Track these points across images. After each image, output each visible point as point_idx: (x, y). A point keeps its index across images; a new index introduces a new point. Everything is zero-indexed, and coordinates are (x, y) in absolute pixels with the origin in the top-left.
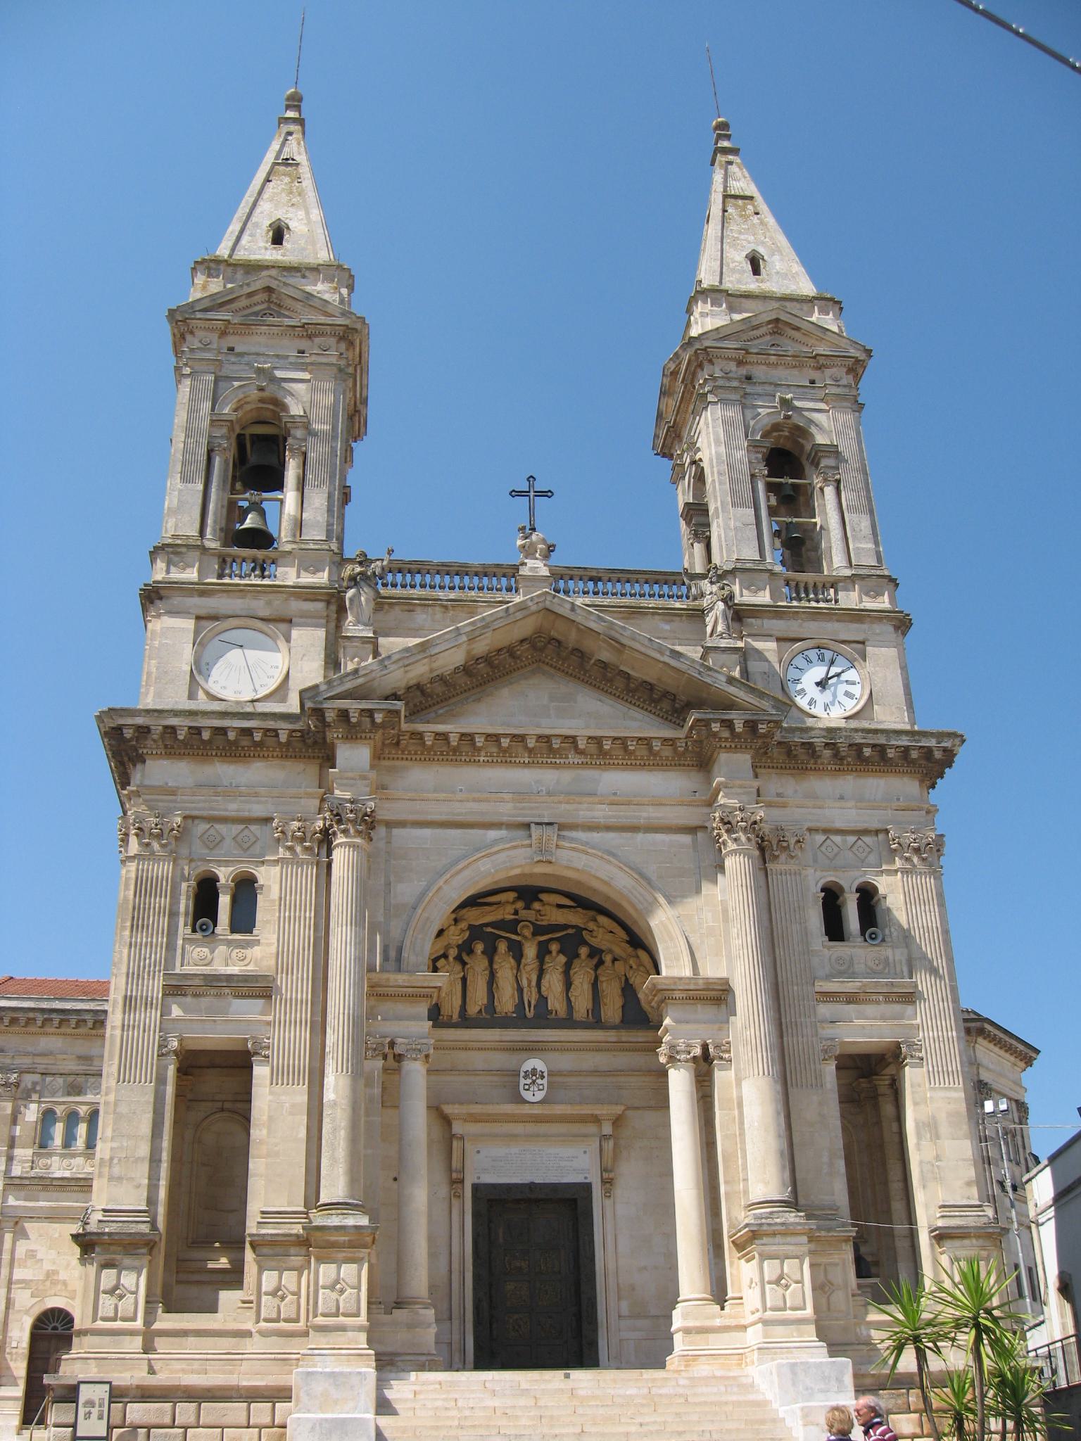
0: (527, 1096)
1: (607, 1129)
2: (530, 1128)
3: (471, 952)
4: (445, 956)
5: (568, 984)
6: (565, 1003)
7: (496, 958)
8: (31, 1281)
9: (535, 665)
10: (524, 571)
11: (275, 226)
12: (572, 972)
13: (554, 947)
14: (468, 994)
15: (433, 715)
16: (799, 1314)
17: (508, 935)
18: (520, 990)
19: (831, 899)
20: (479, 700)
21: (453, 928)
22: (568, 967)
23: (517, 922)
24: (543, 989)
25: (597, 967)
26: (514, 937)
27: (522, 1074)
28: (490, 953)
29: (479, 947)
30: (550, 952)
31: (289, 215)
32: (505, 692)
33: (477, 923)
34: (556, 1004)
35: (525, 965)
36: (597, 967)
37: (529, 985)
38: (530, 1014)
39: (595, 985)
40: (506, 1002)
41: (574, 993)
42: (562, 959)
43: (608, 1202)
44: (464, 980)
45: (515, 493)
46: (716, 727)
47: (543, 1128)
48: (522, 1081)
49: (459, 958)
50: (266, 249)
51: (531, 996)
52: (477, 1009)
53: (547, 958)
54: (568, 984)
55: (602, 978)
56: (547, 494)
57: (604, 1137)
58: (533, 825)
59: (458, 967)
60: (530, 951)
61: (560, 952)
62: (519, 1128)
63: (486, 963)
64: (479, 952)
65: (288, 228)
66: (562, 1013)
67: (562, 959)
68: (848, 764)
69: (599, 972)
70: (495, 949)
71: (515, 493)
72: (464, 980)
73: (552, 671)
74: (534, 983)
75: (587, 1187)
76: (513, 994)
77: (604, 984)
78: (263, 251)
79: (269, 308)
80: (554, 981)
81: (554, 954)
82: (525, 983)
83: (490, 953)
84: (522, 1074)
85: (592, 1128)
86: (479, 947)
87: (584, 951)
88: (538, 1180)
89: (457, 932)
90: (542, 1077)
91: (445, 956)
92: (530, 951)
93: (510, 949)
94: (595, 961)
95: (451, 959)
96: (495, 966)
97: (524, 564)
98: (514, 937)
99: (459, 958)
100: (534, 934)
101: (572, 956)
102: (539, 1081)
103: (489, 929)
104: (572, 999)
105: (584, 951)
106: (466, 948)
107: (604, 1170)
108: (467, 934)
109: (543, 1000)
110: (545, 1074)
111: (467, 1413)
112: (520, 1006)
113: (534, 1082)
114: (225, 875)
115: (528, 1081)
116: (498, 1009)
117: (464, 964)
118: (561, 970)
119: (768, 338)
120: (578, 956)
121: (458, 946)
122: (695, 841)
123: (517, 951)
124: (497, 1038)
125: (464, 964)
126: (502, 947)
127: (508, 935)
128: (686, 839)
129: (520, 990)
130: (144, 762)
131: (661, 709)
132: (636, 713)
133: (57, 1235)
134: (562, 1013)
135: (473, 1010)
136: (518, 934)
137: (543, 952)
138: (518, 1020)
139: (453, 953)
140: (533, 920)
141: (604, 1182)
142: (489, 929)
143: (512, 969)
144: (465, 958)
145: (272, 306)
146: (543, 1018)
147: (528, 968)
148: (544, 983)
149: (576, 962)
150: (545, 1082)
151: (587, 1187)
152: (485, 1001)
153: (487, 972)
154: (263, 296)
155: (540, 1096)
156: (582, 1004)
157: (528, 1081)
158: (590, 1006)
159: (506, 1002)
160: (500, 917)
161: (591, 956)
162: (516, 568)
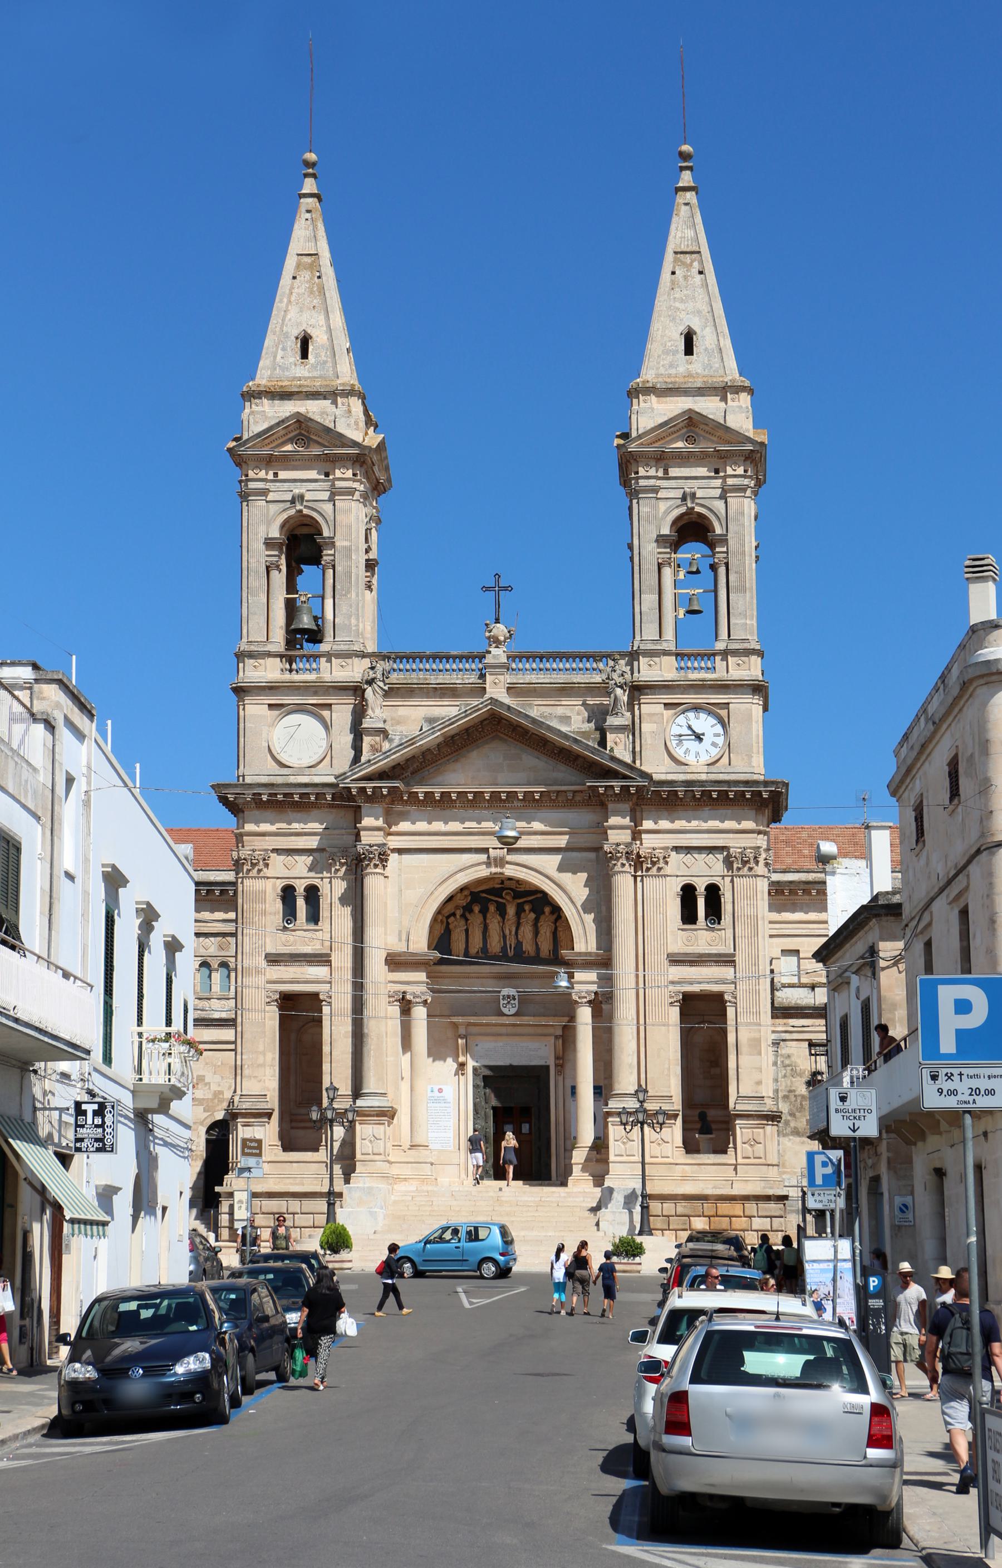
0: (505, 1011)
1: (559, 1032)
2: (510, 1030)
3: (471, 911)
4: (454, 914)
5: (536, 933)
6: (534, 946)
7: (488, 915)
8: (203, 1099)
9: (494, 734)
10: (489, 660)
11: (300, 337)
12: (539, 925)
13: (527, 907)
14: (470, 941)
15: (427, 773)
16: (632, 1159)
17: (497, 899)
18: (504, 937)
19: (688, 893)
20: (456, 761)
21: (459, 895)
22: (537, 920)
23: (503, 889)
24: (519, 937)
25: (556, 920)
26: (500, 900)
27: (501, 997)
28: (484, 912)
29: (476, 909)
30: (525, 911)
31: (313, 321)
32: (474, 754)
33: (476, 890)
34: (528, 947)
35: (508, 920)
36: (556, 920)
37: (510, 934)
38: (511, 953)
39: (555, 934)
40: (495, 945)
41: (540, 939)
42: (533, 916)
43: (561, 1078)
44: (467, 931)
45: (486, 589)
46: (601, 790)
47: (519, 1030)
48: (502, 1002)
49: (463, 916)
50: (295, 365)
51: (511, 941)
52: (476, 950)
53: (523, 915)
54: (536, 933)
55: (559, 929)
56: (507, 589)
57: (557, 1037)
58: (490, 850)
59: (463, 922)
60: (511, 911)
61: (532, 910)
62: (503, 1030)
63: (480, 917)
64: (477, 912)
65: (311, 337)
66: (532, 953)
67: (533, 916)
68: (704, 801)
69: (558, 924)
70: (488, 909)
71: (486, 589)
72: (467, 931)
73: (506, 737)
74: (513, 933)
75: (547, 1068)
76: (500, 940)
77: (561, 933)
78: (293, 367)
79: (300, 434)
80: (526, 932)
81: (527, 911)
82: (507, 932)
83: (484, 912)
84: (501, 997)
85: (551, 1030)
86: (476, 909)
87: (547, 910)
88: (515, 1063)
89: (462, 898)
90: (514, 999)
91: (454, 914)
92: (511, 911)
93: (498, 909)
94: (555, 916)
95: (458, 917)
96: (487, 921)
97: (489, 652)
98: (500, 900)
99: (463, 916)
100: (515, 898)
101: (538, 912)
102: (512, 1002)
103: (484, 895)
104: (539, 943)
105: (547, 910)
106: (468, 909)
107: (557, 1058)
108: (470, 898)
109: (519, 944)
110: (516, 997)
111: (436, 1209)
112: (504, 949)
113: (509, 1002)
114: (300, 886)
115: (506, 1002)
116: (490, 950)
117: (467, 920)
118: (531, 924)
119: (685, 430)
120: (544, 913)
121: (463, 907)
122: (597, 857)
123: (502, 911)
124: (488, 971)
125: (467, 920)
126: (492, 908)
127: (497, 899)
128: (592, 855)
129: (504, 937)
130: (243, 812)
131: (577, 765)
132: (562, 767)
133: (220, 1063)
134: (532, 953)
135: (473, 951)
136: (502, 898)
137: (520, 911)
138: (503, 957)
139: (459, 913)
140: (514, 887)
141: (556, 1065)
142: (484, 895)
143: (499, 923)
144: (467, 915)
145: (303, 432)
146: (520, 957)
147: (510, 922)
148: (520, 932)
149: (542, 917)
150: (516, 1002)
151: (547, 1068)
152: (481, 946)
153: (482, 926)
154: (297, 425)
155: (513, 1011)
156: (546, 947)
157: (506, 1002)
158: (551, 948)
159: (495, 945)
160: (492, 886)
161: (552, 913)
162: (481, 657)
